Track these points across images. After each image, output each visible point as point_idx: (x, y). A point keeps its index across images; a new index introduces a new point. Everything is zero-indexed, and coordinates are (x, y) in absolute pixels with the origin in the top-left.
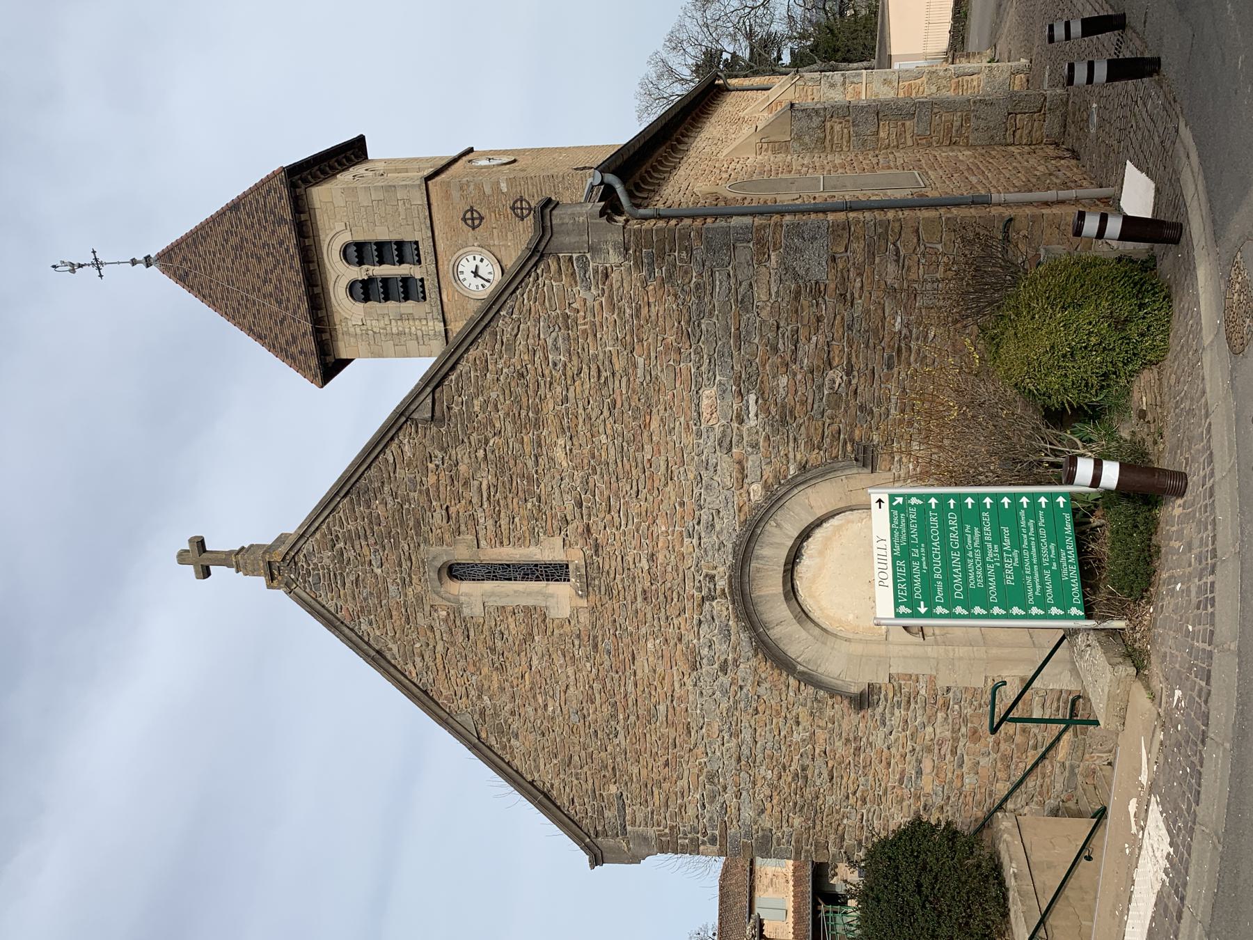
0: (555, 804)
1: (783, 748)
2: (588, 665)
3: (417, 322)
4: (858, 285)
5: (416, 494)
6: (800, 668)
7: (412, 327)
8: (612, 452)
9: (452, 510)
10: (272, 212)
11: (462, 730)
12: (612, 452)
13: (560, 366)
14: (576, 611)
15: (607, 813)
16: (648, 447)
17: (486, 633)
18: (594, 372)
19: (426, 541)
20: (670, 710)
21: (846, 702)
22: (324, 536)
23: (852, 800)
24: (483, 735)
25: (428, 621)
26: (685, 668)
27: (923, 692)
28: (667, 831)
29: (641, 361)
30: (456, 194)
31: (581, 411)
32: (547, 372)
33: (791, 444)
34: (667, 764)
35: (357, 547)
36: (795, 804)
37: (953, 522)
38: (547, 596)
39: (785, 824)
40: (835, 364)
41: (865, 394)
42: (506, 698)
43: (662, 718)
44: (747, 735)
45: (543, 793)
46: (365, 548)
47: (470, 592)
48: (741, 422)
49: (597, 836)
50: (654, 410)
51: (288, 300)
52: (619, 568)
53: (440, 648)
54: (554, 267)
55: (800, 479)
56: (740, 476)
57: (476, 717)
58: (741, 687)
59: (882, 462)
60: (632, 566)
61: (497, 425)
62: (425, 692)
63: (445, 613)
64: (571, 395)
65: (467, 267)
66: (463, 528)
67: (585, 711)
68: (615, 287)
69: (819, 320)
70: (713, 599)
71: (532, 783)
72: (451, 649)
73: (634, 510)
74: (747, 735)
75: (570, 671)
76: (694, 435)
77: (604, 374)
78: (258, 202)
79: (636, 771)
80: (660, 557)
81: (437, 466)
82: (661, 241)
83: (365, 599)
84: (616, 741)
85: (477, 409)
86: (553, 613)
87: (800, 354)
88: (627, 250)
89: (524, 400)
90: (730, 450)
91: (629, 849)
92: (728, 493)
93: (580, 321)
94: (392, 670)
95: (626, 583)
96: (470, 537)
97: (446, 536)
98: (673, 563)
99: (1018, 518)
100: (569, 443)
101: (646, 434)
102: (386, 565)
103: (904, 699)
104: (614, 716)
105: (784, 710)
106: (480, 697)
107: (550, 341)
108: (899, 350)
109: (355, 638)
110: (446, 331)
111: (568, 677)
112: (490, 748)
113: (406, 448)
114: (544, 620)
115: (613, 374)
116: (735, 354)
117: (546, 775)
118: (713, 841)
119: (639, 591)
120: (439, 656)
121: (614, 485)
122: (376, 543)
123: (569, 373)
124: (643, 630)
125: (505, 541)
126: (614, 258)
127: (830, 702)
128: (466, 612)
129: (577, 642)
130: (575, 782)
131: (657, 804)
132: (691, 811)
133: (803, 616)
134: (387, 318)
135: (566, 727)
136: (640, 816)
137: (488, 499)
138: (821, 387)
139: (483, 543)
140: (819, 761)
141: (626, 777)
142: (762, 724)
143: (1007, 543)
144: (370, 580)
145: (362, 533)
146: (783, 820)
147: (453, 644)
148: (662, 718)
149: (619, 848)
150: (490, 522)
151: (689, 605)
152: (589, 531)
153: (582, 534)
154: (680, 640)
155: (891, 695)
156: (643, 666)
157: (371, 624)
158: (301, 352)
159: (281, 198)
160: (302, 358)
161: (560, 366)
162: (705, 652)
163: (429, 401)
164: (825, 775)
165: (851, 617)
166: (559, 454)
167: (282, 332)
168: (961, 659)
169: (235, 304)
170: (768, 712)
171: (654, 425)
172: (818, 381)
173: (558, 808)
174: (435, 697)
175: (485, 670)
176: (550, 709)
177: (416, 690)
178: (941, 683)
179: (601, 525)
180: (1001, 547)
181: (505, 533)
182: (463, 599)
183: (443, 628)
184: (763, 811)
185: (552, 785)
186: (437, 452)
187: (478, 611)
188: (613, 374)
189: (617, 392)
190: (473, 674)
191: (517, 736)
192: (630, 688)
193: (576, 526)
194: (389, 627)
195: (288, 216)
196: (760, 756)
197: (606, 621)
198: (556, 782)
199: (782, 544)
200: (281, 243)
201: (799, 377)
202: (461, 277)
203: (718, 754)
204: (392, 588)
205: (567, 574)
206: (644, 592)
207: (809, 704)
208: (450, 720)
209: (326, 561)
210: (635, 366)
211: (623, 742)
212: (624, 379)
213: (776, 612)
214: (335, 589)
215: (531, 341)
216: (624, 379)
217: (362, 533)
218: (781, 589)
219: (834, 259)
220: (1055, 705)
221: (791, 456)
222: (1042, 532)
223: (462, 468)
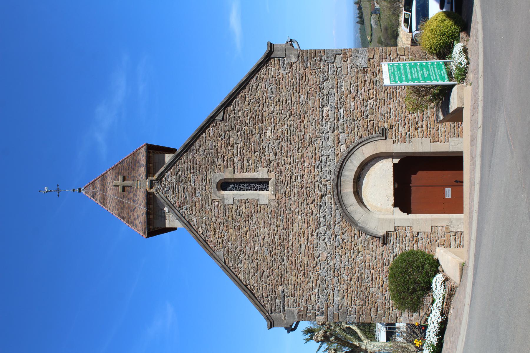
0: (255, 296)
1: (352, 265)
2: (274, 227)
4: (378, 69)
5: (212, 151)
6: (359, 225)
8: (289, 132)
9: (226, 157)
10: (139, 162)
11: (219, 259)
12: (289, 132)
13: (272, 98)
14: (271, 201)
15: (277, 301)
16: (303, 130)
17: (233, 212)
18: (284, 101)
19: (214, 171)
20: (307, 248)
21: (378, 241)
22: (174, 169)
23: (381, 290)
24: (227, 262)
25: (210, 207)
26: (313, 227)
27: (408, 235)
28: (302, 309)
29: (302, 96)
31: (278, 115)
32: (267, 101)
33: (356, 129)
34: (304, 274)
35: (186, 174)
36: (357, 292)
37: (408, 68)
38: (259, 195)
39: (353, 304)
40: (371, 97)
41: (382, 108)
42: (238, 243)
43: (303, 251)
44: (338, 258)
45: (250, 290)
46: (189, 174)
47: (229, 195)
48: (338, 120)
49: (272, 313)
50: (306, 115)
51: (138, 199)
52: (289, 182)
53: (213, 220)
54: (273, 62)
55: (360, 141)
56: (337, 142)
57: (225, 253)
58: (336, 236)
59: (389, 136)
60: (294, 181)
61: (247, 121)
62: (205, 241)
63: (217, 203)
64: (275, 109)
66: (229, 165)
67: (271, 249)
68: (294, 69)
69: (365, 81)
70: (326, 195)
71: (246, 286)
72: (218, 220)
73: (296, 157)
74: (338, 258)
75: (266, 230)
76: (320, 125)
77: (288, 102)
78: (133, 159)
79: (290, 278)
80: (306, 176)
81: (222, 139)
82: (311, 53)
83: (186, 197)
84: (283, 263)
85: (240, 115)
86: (261, 203)
87: (359, 94)
88: (299, 56)
89: (258, 111)
90: (333, 132)
91: (285, 319)
92: (333, 149)
93: (281, 82)
94: (192, 230)
95: (292, 188)
96: (232, 169)
97: (222, 169)
98: (310, 179)
99: (428, 67)
100: (273, 128)
101: (302, 125)
102: (196, 182)
103: (401, 239)
104: (283, 251)
105: (353, 245)
106: (227, 243)
107: (269, 89)
108: (393, 92)
109: (179, 215)
111: (265, 232)
112: (229, 268)
113: (211, 132)
114: (257, 206)
115: (292, 101)
116: (336, 94)
117: (253, 282)
118: (322, 313)
119: (296, 192)
120: (212, 223)
121: (289, 146)
122: (194, 172)
123: (275, 101)
124: (297, 210)
125: (245, 171)
126: (294, 59)
127: (371, 241)
128: (226, 202)
129: (270, 216)
130: (264, 285)
131: (298, 295)
132: (313, 299)
133: (360, 201)
135: (262, 257)
136: (291, 302)
137: (240, 152)
138: (366, 106)
139: (236, 171)
140: (367, 271)
141: (286, 282)
142: (344, 253)
143: (425, 70)
144: (190, 189)
145: (189, 168)
146: (352, 302)
147: (219, 217)
148: (303, 251)
149: (281, 319)
150: (240, 162)
151: (316, 198)
152: (278, 165)
153: (275, 167)
154: (312, 214)
155: (395, 237)
156: (296, 227)
157: (187, 209)
158: (139, 223)
159: (143, 156)
160: (140, 225)
161: (272, 98)
162: (321, 219)
163: (222, 112)
164: (370, 278)
165: (379, 205)
166: (269, 133)
167: (133, 215)
168: (421, 219)
169: (114, 204)
170: (346, 247)
171: (306, 121)
172: (365, 104)
173: (256, 298)
174: (209, 244)
175: (231, 230)
176: (256, 248)
177: (201, 240)
178: (415, 230)
179: (283, 163)
180: (423, 72)
181: (245, 167)
182: (225, 196)
183: (216, 210)
184: (343, 298)
185: (254, 287)
186: (222, 133)
187: (231, 202)
188: (292, 101)
189: (293, 108)
190: (226, 232)
191: (241, 262)
192: (290, 236)
193: (274, 163)
194: (194, 210)
195: (145, 163)
196: (343, 269)
197: (283, 205)
198: (256, 285)
199: (352, 170)
200: (139, 175)
201: (358, 102)
203: (326, 269)
204: (197, 192)
205: (268, 188)
206: (298, 192)
207: (363, 242)
208: (214, 254)
209: (173, 180)
210: (300, 98)
211: (286, 264)
212: (295, 103)
213: (350, 199)
214: (175, 193)
215: (262, 89)
216: (295, 103)
217: (189, 168)
218: (352, 190)
219: (369, 61)
220: (459, 239)
221: (356, 133)
222: (436, 69)
223: (231, 139)
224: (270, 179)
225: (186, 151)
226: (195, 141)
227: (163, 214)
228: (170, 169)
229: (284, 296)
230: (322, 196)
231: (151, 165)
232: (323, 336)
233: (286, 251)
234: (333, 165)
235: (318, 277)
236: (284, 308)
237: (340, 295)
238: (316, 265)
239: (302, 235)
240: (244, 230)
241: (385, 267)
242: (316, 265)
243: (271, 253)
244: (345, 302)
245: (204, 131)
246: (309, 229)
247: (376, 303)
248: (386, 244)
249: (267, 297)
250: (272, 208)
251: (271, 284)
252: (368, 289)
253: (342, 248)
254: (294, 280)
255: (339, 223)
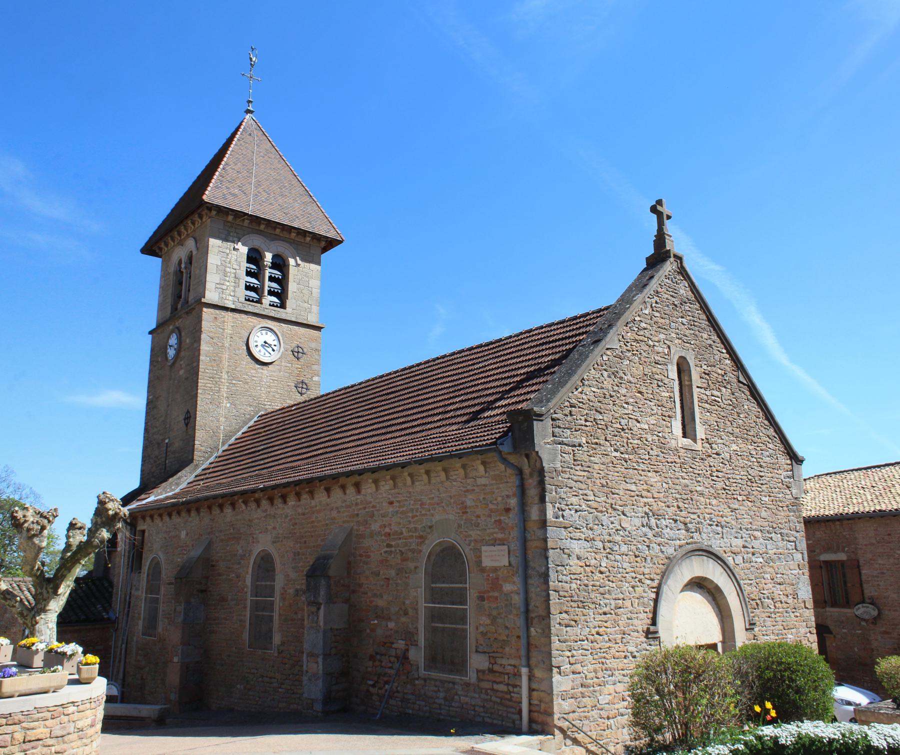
3: (232, 288)
7: (229, 284)
30: (313, 345)
39: (573, 577)
49: (553, 420)
65: (270, 338)
74: (624, 549)
110: (226, 309)
120: (646, 339)
132: (574, 500)
134: (237, 267)
202: (264, 332)
224: (695, 440)
225: (709, 320)
226: (719, 336)
227: (231, 239)
228: (691, 290)
229: (574, 446)
230: (685, 524)
231: (308, 239)
232: (116, 514)
233: (627, 456)
234: (717, 545)
235: (602, 512)
236: (560, 444)
237: (582, 553)
238: (615, 510)
239: (645, 487)
240: (643, 390)
241: (620, 636)
242: (615, 510)
243: (623, 429)
244: (573, 561)
245: (728, 352)
246: (652, 500)
247: (576, 621)
248: (647, 637)
249: (571, 415)
250: (668, 440)
251: (588, 424)
252: (593, 606)
253: (636, 557)
254: (596, 466)
255: (663, 552)
